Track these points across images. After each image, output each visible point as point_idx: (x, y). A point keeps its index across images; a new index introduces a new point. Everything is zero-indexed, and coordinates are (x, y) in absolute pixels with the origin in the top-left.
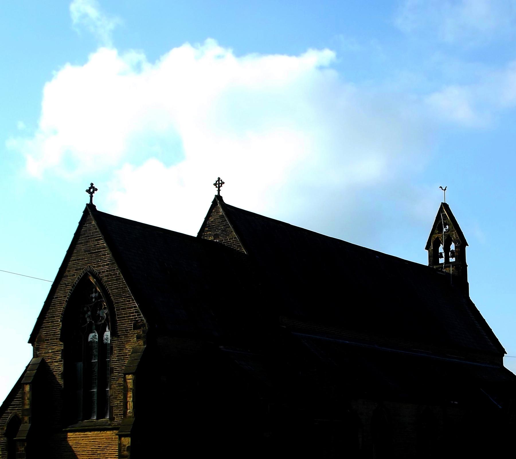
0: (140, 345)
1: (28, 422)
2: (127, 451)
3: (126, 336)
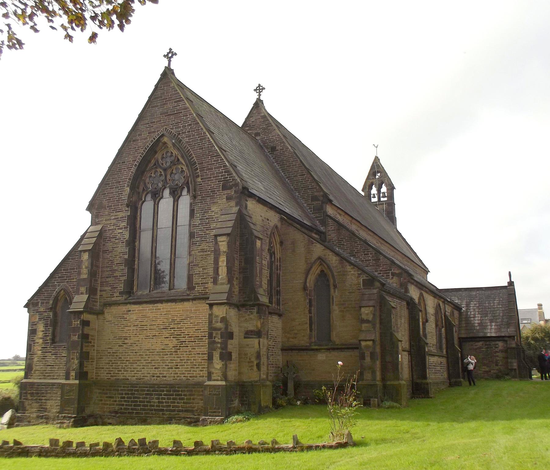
2: (220, 322)
3: (212, 197)
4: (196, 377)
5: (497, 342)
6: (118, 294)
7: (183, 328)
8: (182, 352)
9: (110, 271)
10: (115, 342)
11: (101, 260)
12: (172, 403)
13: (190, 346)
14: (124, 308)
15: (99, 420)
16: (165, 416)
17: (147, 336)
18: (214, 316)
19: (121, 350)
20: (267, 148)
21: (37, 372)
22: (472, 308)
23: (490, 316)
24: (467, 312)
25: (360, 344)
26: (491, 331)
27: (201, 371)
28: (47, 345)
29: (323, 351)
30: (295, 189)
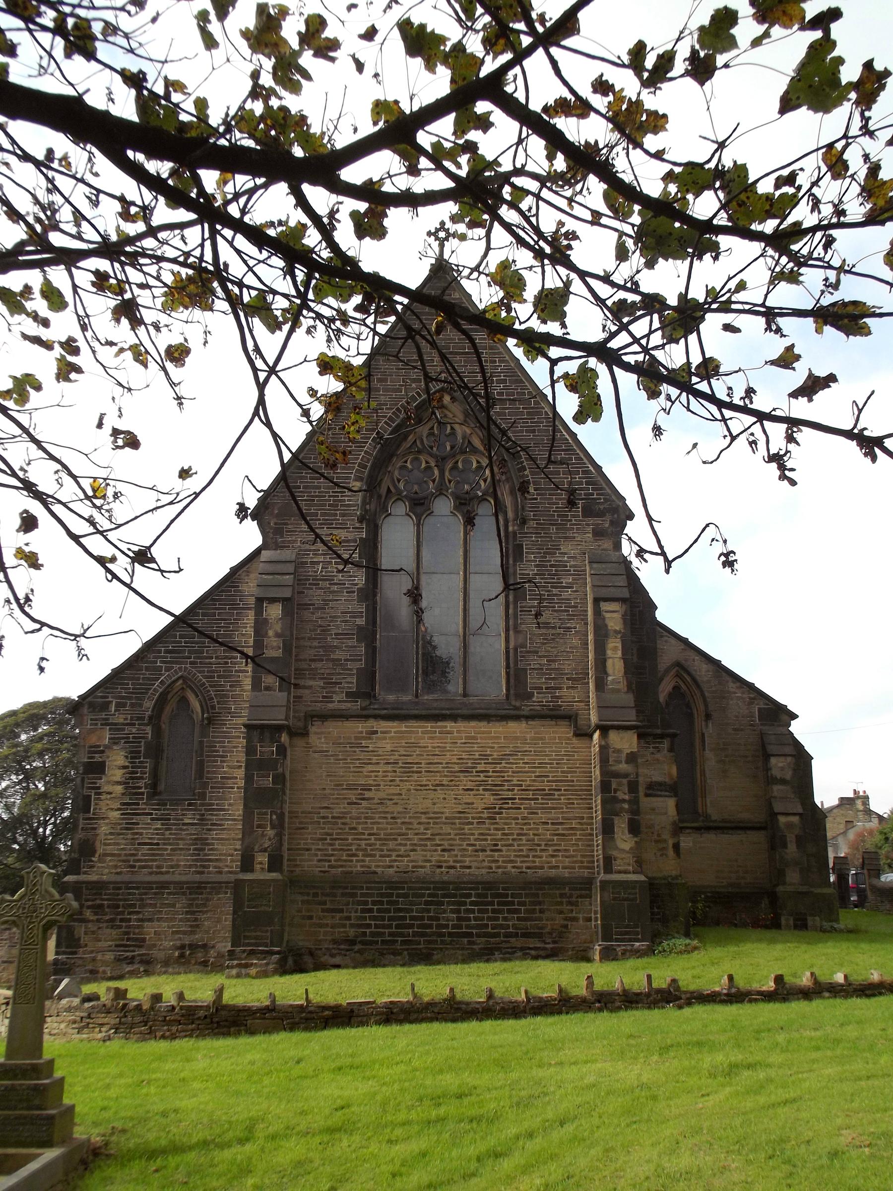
2: (627, 762)
3: (561, 527)
4: (542, 868)
7: (508, 772)
8: (507, 818)
9: (320, 647)
10: (338, 794)
12: (489, 919)
13: (525, 808)
14: (361, 727)
15: (307, 959)
16: (474, 947)
17: (421, 786)
18: (611, 750)
19: (354, 812)
21: (109, 858)
27: (553, 856)
28: (137, 799)
29: (688, 831)
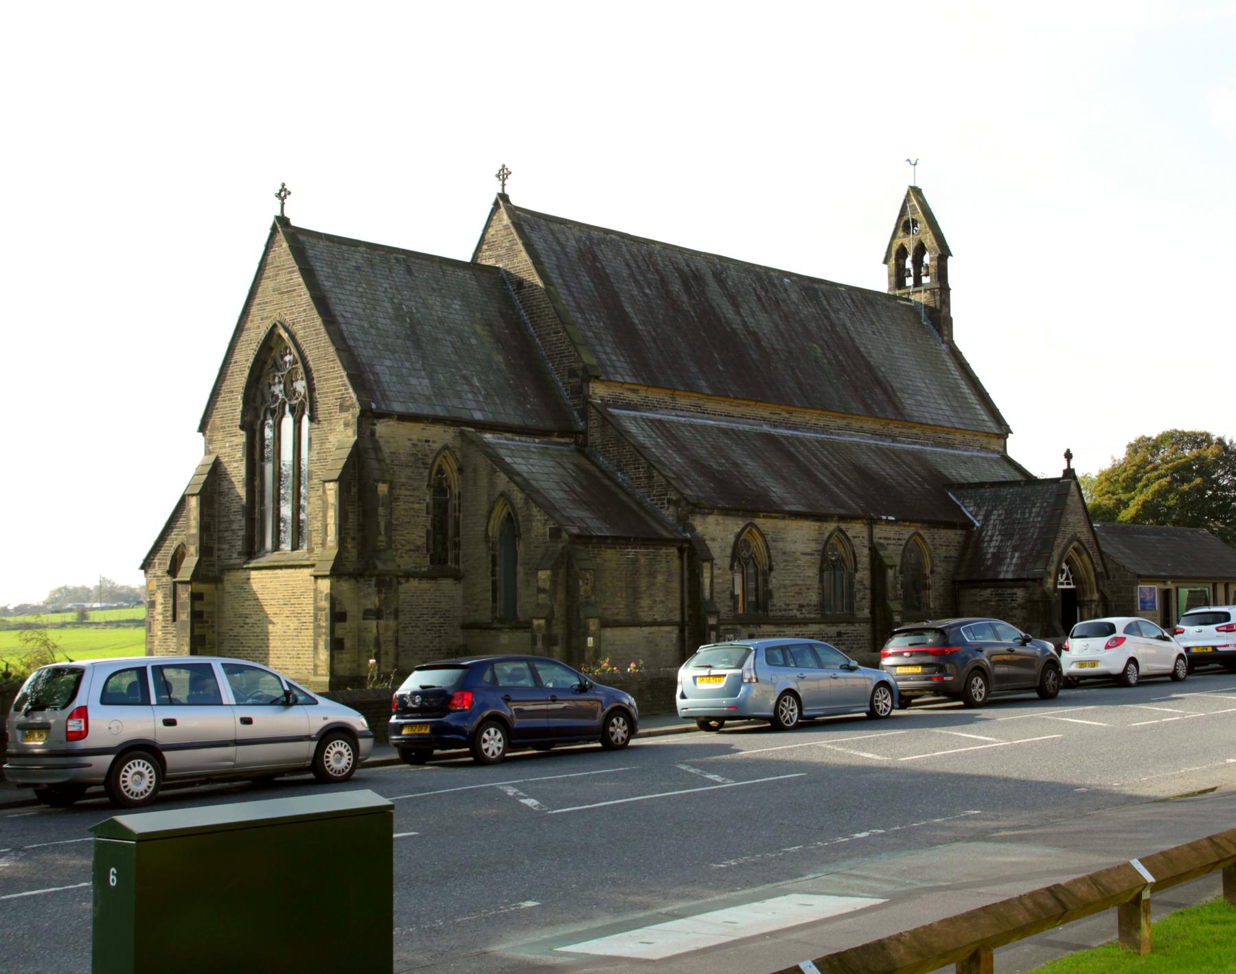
0: (348, 437)
1: (194, 554)
5: (1016, 590)
6: (235, 555)
11: (216, 506)
20: (512, 283)
22: (992, 522)
23: (1015, 540)
24: (981, 529)
25: (532, 623)
26: (1007, 571)
30: (548, 356)
